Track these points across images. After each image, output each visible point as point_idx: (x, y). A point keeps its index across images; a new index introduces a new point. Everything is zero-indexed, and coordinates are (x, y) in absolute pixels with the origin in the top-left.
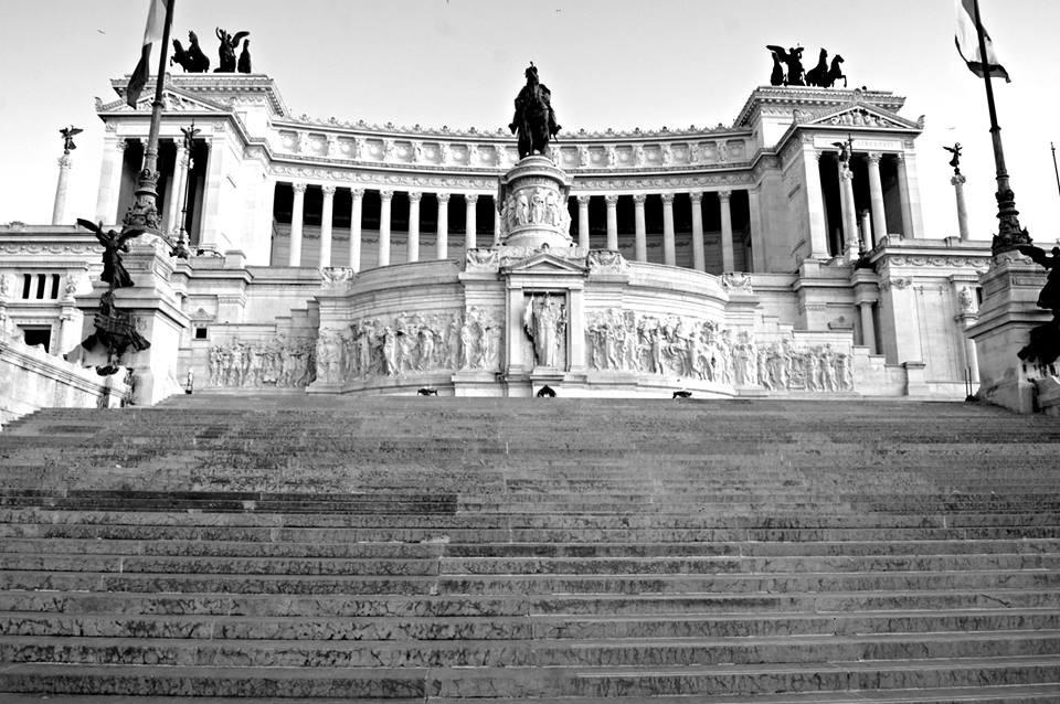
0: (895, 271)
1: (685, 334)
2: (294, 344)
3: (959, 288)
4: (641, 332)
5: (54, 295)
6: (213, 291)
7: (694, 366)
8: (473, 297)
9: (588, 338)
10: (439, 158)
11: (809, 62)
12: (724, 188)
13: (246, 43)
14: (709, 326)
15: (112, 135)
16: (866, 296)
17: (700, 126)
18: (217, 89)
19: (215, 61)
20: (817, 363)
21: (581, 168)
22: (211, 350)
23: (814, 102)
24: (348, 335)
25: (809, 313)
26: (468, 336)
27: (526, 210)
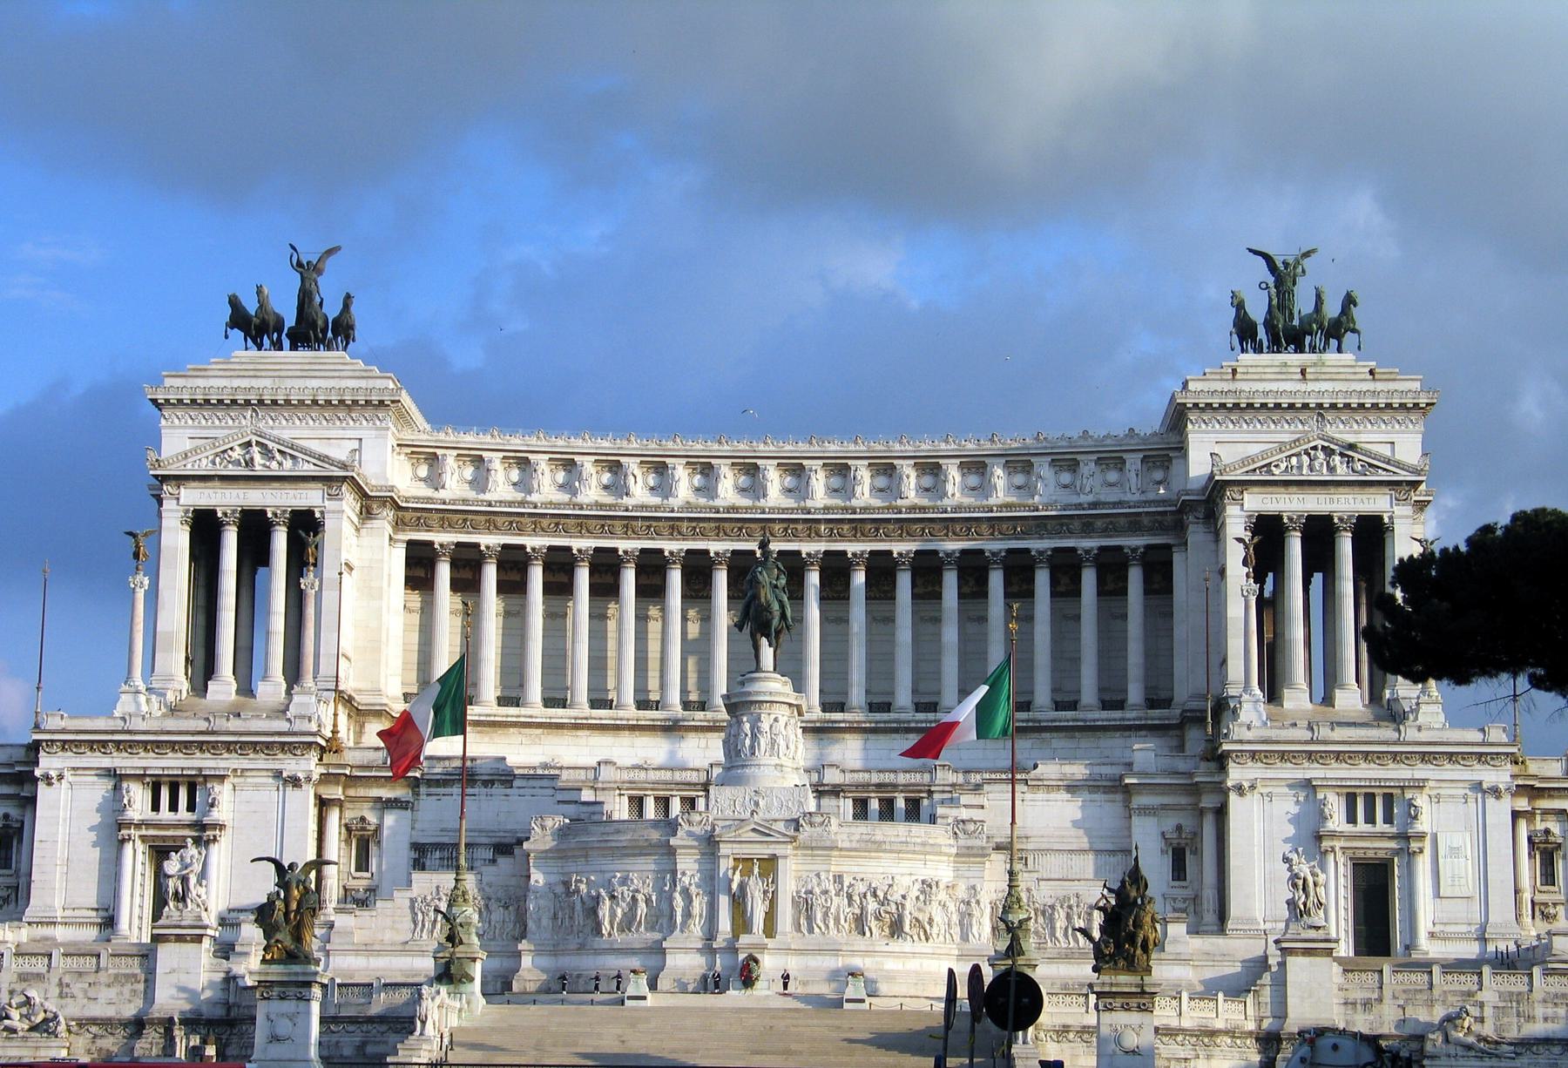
0: (1236, 774)
1: (896, 897)
2: (500, 894)
3: (1320, 796)
4: (850, 897)
5: (191, 807)
7: (907, 928)
11: (1303, 304)
13: (348, 297)
14: (927, 886)
16: (1208, 801)
18: (315, 402)
19: (290, 321)
20: (1063, 914)
21: (899, 502)
22: (413, 901)
23: (1278, 406)
24: (560, 889)
25: (1136, 821)
26: (679, 902)
27: (748, 742)
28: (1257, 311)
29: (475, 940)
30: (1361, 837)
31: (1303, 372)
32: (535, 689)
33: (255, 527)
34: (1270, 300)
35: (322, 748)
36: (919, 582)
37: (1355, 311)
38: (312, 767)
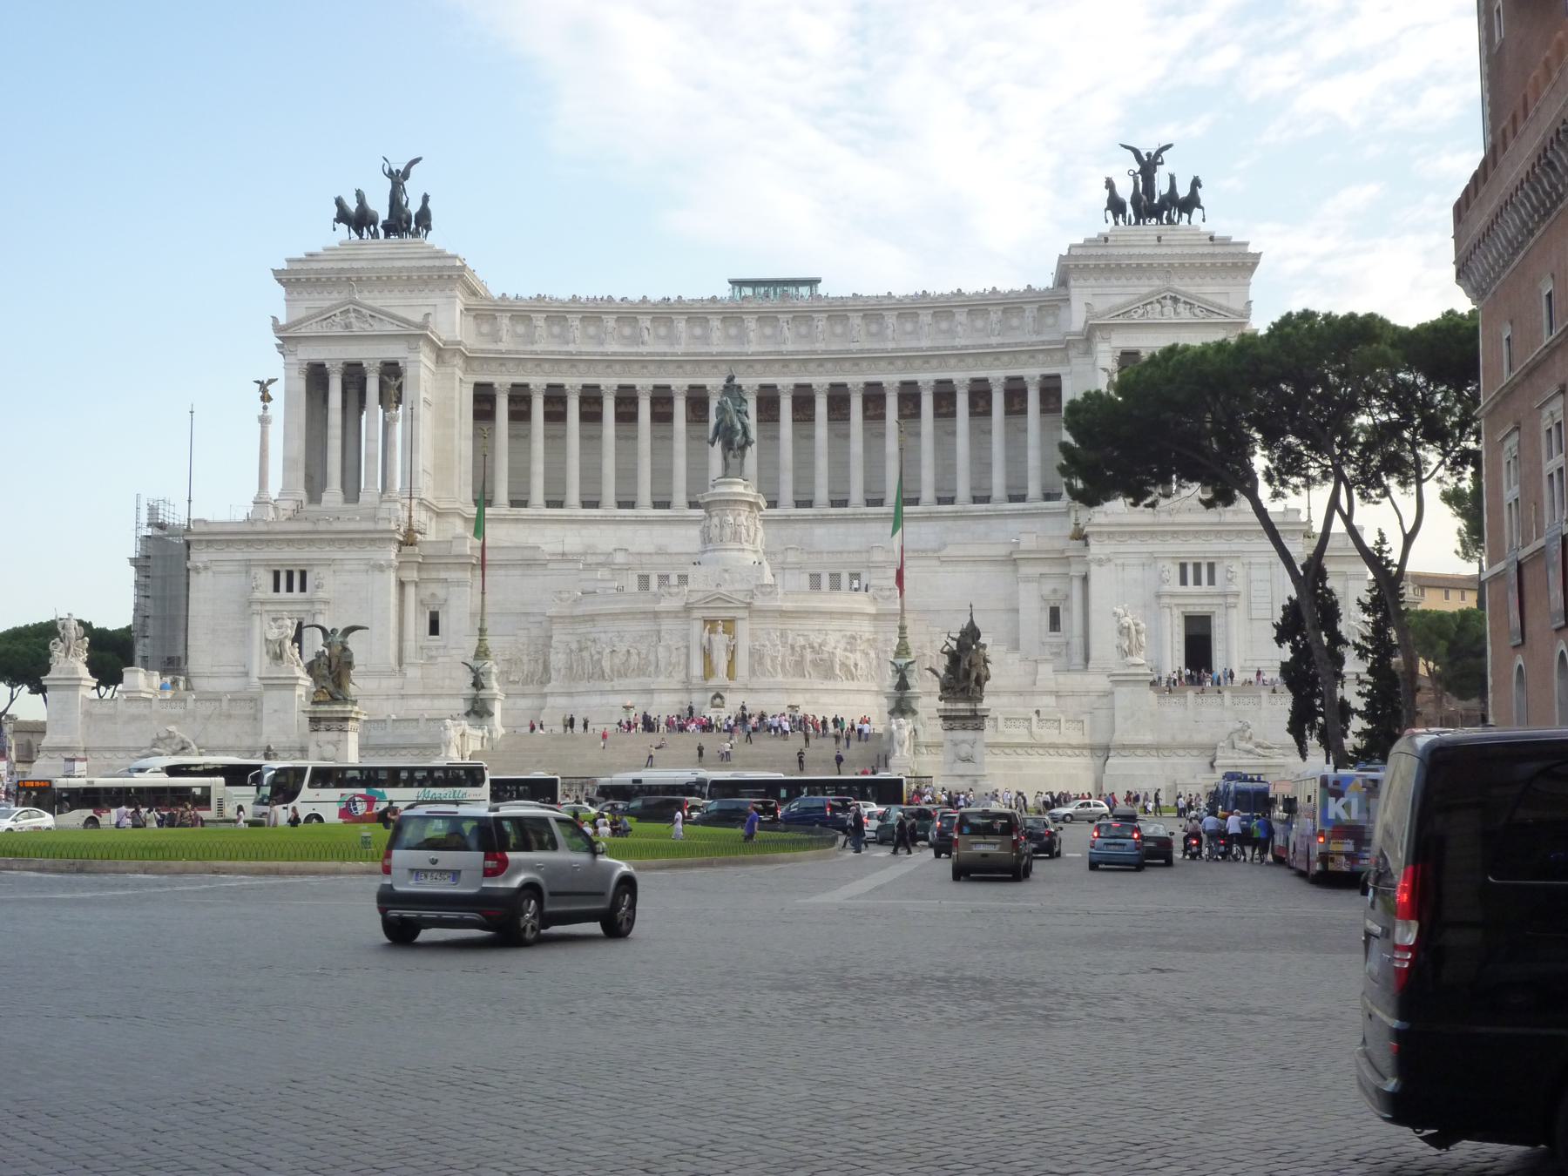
0: (1096, 549)
2: (532, 648)
3: (1160, 565)
4: (793, 647)
5: (303, 588)
6: (443, 575)
8: (667, 625)
9: (751, 654)
10: (672, 338)
11: (1161, 186)
12: (1032, 373)
13: (426, 198)
15: (292, 359)
16: (1076, 570)
17: (1004, 287)
19: (383, 214)
23: (1138, 265)
24: (574, 646)
28: (1125, 191)
29: (495, 684)
30: (1190, 596)
31: (1159, 239)
32: (573, 495)
33: (354, 376)
34: (1136, 184)
35: (401, 543)
36: (871, 405)
37: (1200, 192)
38: (393, 556)
